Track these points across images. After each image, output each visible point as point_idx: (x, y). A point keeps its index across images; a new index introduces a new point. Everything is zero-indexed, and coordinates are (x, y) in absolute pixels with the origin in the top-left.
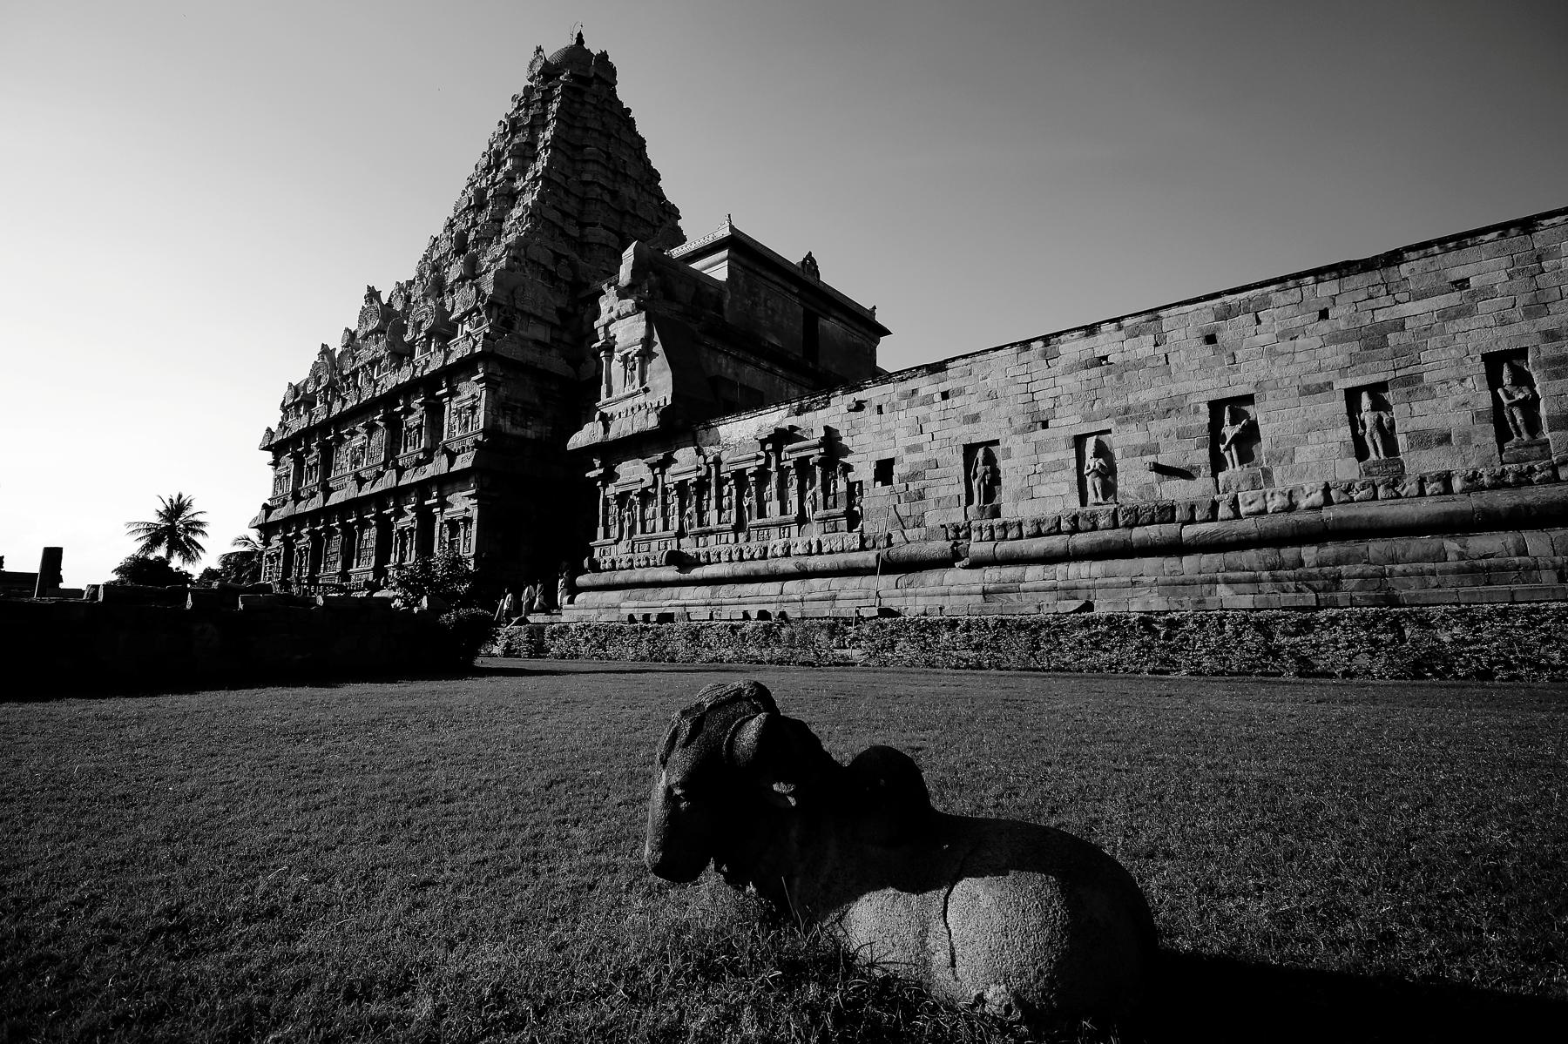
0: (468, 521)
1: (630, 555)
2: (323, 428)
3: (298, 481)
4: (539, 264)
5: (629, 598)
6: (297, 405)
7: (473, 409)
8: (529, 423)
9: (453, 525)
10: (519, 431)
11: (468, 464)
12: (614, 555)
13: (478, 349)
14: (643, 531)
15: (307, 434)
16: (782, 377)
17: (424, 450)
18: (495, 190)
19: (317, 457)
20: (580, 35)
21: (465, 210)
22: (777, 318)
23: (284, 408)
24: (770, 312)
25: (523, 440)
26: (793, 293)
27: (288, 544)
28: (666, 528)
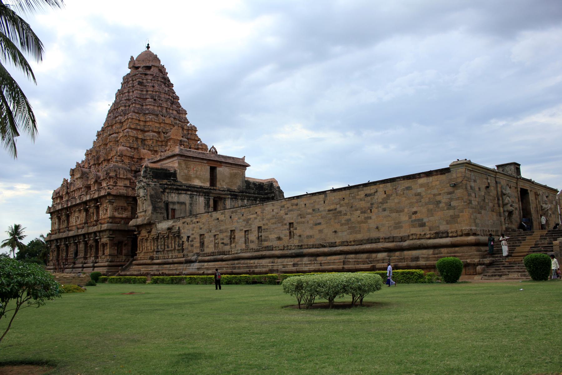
0: (106, 244)
1: (143, 257)
2: (67, 209)
3: (59, 225)
4: (127, 156)
5: (142, 268)
6: (57, 198)
7: (107, 210)
8: (124, 212)
9: (104, 245)
10: (120, 216)
11: (105, 228)
12: (141, 256)
13: (106, 194)
14: (147, 250)
15: (61, 210)
16: (196, 195)
17: (95, 221)
18: (116, 121)
19: (65, 218)
20: (148, 45)
21: (107, 127)
22: (198, 173)
23: (53, 198)
24: (195, 172)
25: (122, 218)
26: (205, 163)
27: (58, 247)
28: (151, 249)
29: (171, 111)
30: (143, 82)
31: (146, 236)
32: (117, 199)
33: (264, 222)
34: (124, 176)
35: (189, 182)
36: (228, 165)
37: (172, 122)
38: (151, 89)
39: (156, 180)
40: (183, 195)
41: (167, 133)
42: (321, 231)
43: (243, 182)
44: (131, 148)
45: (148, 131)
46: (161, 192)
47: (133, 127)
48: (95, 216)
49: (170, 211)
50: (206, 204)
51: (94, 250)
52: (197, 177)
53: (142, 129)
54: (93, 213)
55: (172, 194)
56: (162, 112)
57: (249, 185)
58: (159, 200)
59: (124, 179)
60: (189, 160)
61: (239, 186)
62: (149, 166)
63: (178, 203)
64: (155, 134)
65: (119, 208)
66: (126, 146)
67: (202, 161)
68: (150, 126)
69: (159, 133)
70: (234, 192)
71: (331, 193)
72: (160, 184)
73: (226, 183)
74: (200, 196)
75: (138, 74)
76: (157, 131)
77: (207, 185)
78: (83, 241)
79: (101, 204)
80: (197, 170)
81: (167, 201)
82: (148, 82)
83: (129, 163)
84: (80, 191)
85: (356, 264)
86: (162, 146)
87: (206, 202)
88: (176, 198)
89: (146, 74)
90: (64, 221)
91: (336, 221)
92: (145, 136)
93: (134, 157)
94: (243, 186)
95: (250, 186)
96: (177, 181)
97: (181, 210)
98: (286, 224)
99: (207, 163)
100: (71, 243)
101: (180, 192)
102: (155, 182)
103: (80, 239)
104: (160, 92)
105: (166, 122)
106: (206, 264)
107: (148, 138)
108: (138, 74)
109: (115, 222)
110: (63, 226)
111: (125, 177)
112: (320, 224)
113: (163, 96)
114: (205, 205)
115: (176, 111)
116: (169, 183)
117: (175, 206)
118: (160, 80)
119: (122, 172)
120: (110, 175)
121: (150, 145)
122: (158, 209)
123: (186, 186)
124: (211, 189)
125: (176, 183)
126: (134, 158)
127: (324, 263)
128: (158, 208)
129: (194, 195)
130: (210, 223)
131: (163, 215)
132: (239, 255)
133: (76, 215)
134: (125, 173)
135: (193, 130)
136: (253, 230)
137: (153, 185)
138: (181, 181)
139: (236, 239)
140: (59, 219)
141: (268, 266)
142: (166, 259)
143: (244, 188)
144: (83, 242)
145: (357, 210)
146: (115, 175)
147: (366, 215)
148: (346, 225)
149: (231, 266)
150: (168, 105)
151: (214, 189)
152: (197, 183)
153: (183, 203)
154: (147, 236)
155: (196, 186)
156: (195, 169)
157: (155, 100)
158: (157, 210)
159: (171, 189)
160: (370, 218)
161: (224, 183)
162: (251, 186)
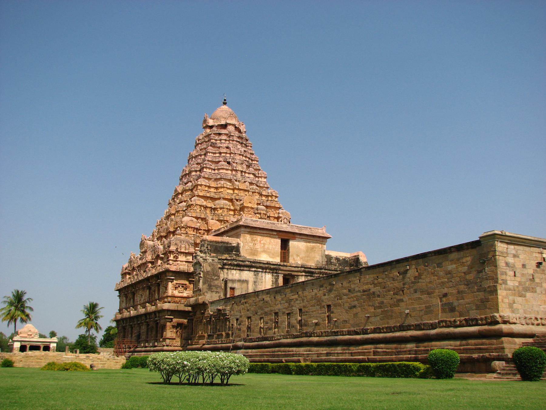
8: (185, 291)
10: (180, 295)
22: (266, 246)
24: (262, 245)
26: (275, 235)
27: (124, 328)
29: (247, 175)
30: (216, 143)
31: (200, 318)
32: (177, 275)
33: (304, 304)
34: (186, 250)
35: (255, 256)
36: (303, 237)
37: (247, 188)
38: (225, 150)
39: (215, 255)
40: (246, 272)
41: (240, 200)
42: (356, 315)
43: (322, 257)
44: (197, 218)
45: (219, 199)
46: (220, 268)
47: (201, 194)
48: (156, 295)
49: (228, 289)
50: (274, 282)
51: (154, 333)
52: (265, 251)
53: (212, 196)
54: (155, 291)
55: (233, 271)
56: (235, 176)
57: (331, 260)
58: (216, 277)
59: (186, 253)
60: (255, 231)
61: (318, 261)
62: (208, 239)
63: (239, 281)
64: (227, 202)
65: (179, 286)
66: (192, 217)
67: (271, 233)
68: (221, 193)
69: (231, 200)
70: (310, 268)
71: (366, 270)
72: (219, 259)
73: (301, 258)
74: (267, 273)
75: (211, 134)
76: (229, 198)
77: (277, 260)
78: (145, 322)
79: (161, 282)
80: (265, 243)
81: (227, 278)
82: (221, 143)
83: (194, 235)
84: (144, 266)
85: (384, 355)
86: (234, 215)
87: (274, 280)
88: (237, 275)
89: (220, 134)
90: (130, 299)
91: (371, 303)
92: (215, 204)
93: (201, 228)
94: (322, 262)
95: (332, 261)
96: (240, 256)
97: (242, 289)
98: (324, 307)
99: (276, 235)
100: (135, 325)
101: (242, 268)
102: (213, 257)
103: (142, 319)
104: (235, 154)
105: (240, 188)
106: (250, 350)
107: (218, 207)
108: (211, 134)
109: (174, 301)
110: (129, 305)
111: (187, 251)
112: (355, 307)
113: (238, 157)
114: (273, 283)
115: (253, 174)
116: (230, 258)
117: (235, 284)
118: (235, 139)
119: (183, 246)
120: (170, 248)
121: (220, 215)
122: (214, 288)
123: (250, 262)
124: (280, 265)
125: (237, 258)
126: (200, 230)
127: (355, 353)
128: (213, 286)
129: (259, 272)
130: (257, 304)
131: (219, 294)
132: (281, 341)
133: (141, 292)
134: (187, 246)
135: (273, 196)
136: (294, 313)
137: (210, 261)
138: (245, 255)
139: (279, 323)
140: (127, 297)
141: (303, 354)
142: (216, 344)
143: (324, 263)
144: (145, 324)
145: (389, 291)
146: (175, 249)
147: (398, 297)
148: (379, 309)
149: (272, 353)
150: (243, 168)
151: (284, 266)
152: (264, 258)
153: (246, 282)
154: (201, 318)
155: (262, 262)
156: (262, 242)
157: (229, 163)
158: (212, 289)
159: (230, 265)
160: (402, 300)
161: (298, 258)
162: (333, 261)
